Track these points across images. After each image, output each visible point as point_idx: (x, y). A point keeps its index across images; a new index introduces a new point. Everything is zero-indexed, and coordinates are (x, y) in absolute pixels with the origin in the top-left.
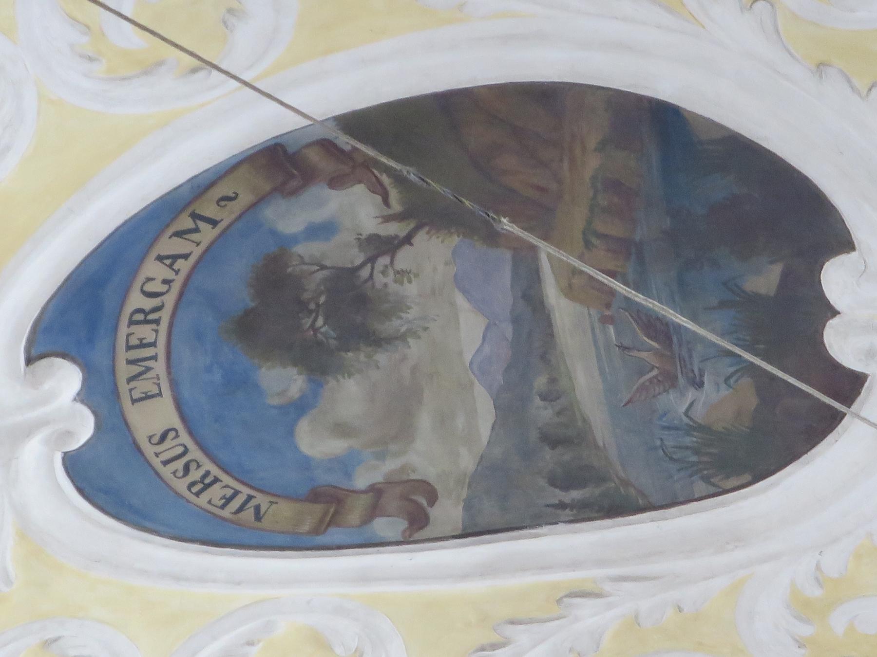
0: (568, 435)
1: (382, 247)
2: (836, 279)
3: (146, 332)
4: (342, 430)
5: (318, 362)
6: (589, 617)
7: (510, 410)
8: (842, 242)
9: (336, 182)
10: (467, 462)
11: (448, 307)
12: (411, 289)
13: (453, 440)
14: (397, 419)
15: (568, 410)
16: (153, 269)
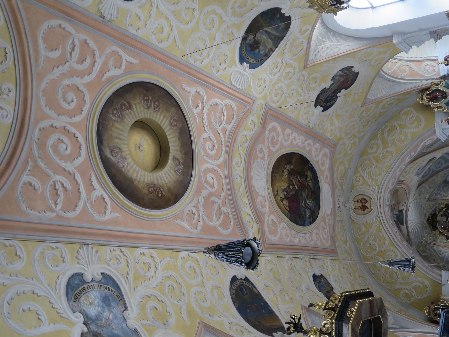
0: (276, 37)
1: (255, 38)
2: (283, 12)
4: (263, 50)
5: (258, 48)
6: (287, 46)
7: (271, 39)
8: (281, 9)
10: (272, 44)
11: (262, 37)
12: (259, 38)
13: (270, 45)
14: (265, 46)
16: (243, 53)
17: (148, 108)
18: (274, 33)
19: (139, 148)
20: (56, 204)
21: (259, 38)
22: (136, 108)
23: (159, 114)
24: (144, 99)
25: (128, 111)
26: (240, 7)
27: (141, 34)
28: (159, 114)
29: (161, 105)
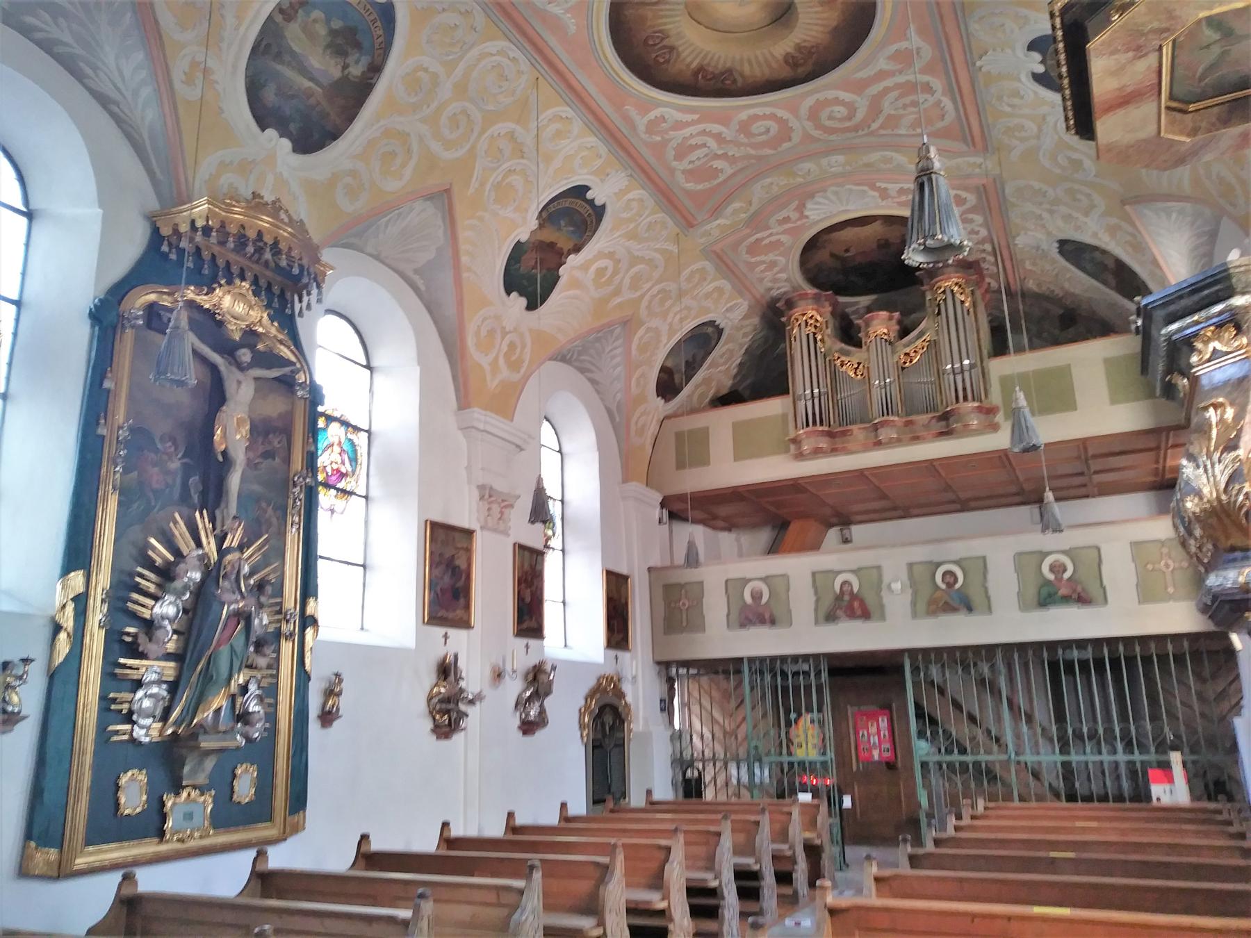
1: (345, 67)
3: (372, 17)
4: (315, 21)
5: (333, 33)
9: (363, 73)
10: (287, 34)
12: (333, 62)
15: (282, 63)
16: (381, 32)
17: (672, 49)
18: (289, 73)
21: (333, 62)
24: (668, 61)
26: (393, 154)
27: (592, 140)
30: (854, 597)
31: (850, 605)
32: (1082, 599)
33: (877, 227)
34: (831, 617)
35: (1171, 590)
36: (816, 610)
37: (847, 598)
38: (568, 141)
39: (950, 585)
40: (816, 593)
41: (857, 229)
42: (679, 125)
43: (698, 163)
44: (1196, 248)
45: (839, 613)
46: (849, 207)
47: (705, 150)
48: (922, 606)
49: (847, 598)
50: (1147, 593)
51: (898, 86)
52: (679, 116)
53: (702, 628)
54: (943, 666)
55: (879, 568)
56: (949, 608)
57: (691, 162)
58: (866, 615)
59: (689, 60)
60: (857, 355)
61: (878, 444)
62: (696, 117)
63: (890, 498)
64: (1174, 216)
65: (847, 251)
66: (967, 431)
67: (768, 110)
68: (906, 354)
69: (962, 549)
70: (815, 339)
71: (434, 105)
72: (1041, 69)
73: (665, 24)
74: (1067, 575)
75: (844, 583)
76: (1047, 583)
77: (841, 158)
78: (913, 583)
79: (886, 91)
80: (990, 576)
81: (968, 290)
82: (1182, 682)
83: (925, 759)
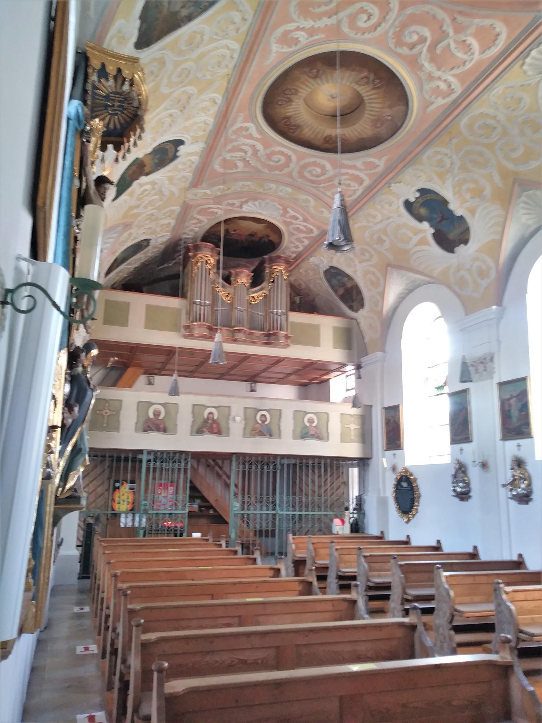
19: (333, 98)
20: (354, 187)
22: (290, 112)
23: (301, 90)
25: (292, 120)
28: (301, 90)
29: (289, 88)
30: (214, 421)
31: (210, 426)
32: (319, 437)
33: (260, 226)
34: (200, 432)
35: (353, 438)
36: (192, 426)
37: (210, 422)
38: (203, 114)
39: (263, 422)
40: (193, 417)
41: (253, 223)
42: (250, 137)
43: (233, 159)
44: (401, 294)
45: (205, 429)
46: (264, 213)
47: (242, 154)
48: (248, 431)
49: (210, 422)
50: (344, 439)
51: (353, 175)
52: (256, 135)
53: (117, 429)
54: (239, 463)
55: (229, 407)
56: (261, 434)
57: (231, 156)
58: (219, 433)
59: (290, 110)
60: (230, 289)
61: (235, 341)
62: (259, 137)
63: (197, 366)
64: (405, 278)
65: (235, 231)
66: (278, 345)
67: (289, 153)
68: (253, 297)
69: (224, 401)
70: (209, 272)
71: (186, 57)
72: (412, 200)
73: (303, 89)
74: (314, 425)
75: (211, 413)
76: (306, 427)
77: (289, 190)
78: (246, 419)
79: (347, 174)
80: (283, 420)
81: (196, 259)
82: (307, 475)
83: (236, 512)
